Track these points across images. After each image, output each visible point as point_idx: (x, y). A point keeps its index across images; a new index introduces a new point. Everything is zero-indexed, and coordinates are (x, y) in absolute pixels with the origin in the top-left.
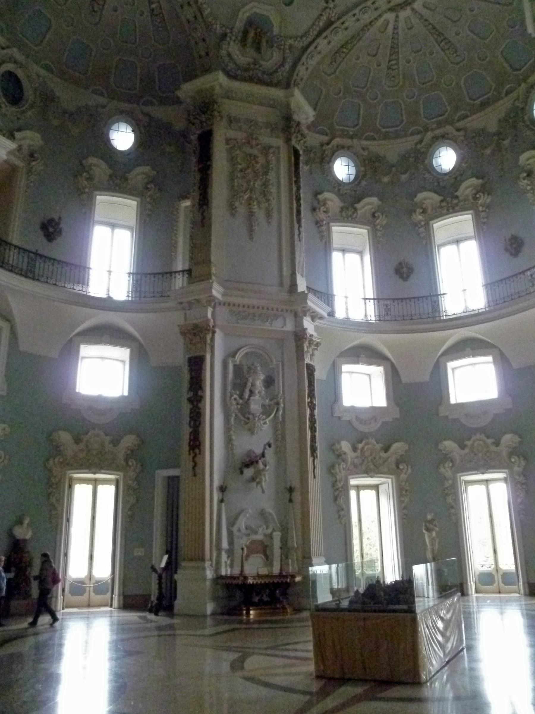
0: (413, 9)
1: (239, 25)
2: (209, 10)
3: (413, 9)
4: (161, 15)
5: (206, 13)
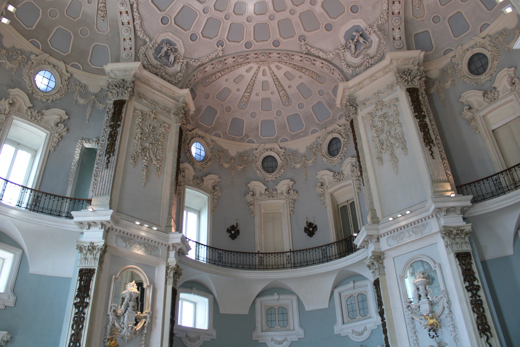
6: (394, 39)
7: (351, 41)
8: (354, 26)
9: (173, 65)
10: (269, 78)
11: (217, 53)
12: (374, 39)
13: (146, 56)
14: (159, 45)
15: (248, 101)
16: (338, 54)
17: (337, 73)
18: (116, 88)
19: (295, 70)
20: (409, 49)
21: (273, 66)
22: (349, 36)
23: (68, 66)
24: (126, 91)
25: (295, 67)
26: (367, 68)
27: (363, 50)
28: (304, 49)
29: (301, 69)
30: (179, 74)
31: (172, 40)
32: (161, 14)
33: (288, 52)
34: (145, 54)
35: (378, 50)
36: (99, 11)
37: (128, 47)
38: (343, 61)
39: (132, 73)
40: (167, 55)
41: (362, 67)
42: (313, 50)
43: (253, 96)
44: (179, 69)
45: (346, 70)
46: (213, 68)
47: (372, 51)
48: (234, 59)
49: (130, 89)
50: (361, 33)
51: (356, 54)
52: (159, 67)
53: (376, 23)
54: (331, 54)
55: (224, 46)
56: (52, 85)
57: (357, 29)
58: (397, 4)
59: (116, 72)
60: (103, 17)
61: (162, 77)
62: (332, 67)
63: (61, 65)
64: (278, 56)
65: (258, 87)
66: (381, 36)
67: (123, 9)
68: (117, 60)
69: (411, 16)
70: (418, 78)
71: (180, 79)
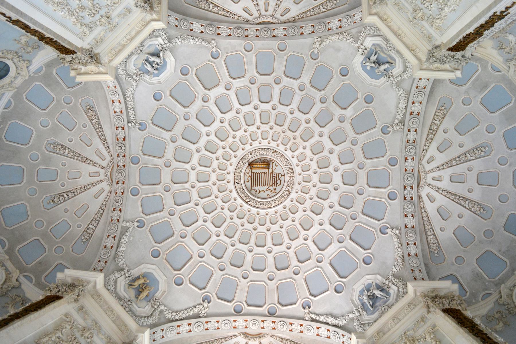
1: (136, 272)
4: (90, 235)
5: (121, 249)
9: (388, 293)
10: (446, 173)
11: (395, 236)
12: (369, 42)
15: (479, 204)
21: (428, 167)
22: (371, 74)
25: (430, 140)
27: (385, 54)
28: (398, 128)
29: (433, 131)
30: (400, 290)
33: (404, 148)
34: (362, 324)
40: (373, 298)
43: (475, 196)
44: (396, 288)
46: (415, 244)
51: (392, 62)
58: (330, 26)
64: (410, 160)
65: (459, 189)
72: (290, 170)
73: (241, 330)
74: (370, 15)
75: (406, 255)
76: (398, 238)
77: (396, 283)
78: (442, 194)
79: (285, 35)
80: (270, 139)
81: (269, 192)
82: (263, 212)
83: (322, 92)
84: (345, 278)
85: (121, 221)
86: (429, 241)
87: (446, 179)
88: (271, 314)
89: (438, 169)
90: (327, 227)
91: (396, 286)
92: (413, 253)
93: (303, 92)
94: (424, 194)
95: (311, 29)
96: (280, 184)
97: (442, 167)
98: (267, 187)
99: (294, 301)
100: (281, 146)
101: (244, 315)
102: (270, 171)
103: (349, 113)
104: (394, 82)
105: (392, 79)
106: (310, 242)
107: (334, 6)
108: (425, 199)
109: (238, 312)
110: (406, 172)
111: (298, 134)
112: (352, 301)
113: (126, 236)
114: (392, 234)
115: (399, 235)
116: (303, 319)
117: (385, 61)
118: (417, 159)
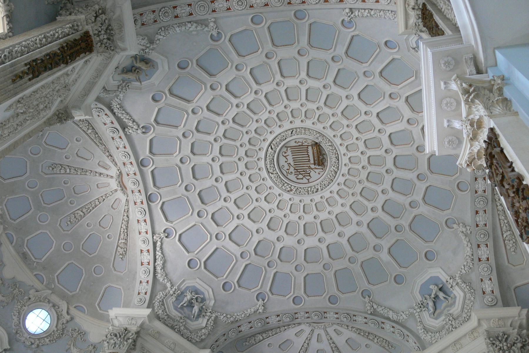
0: (116, 191)
1: (153, 56)
2: (179, 32)
3: (116, 191)
6: (484, 293)
7: (428, 297)
8: (431, 277)
12: (458, 293)
13: (163, 304)
14: (182, 293)
16: (412, 315)
17: (412, 339)
18: (115, 338)
19: (359, 336)
20: (506, 304)
21: (330, 330)
22: (424, 289)
23: (71, 308)
24: (125, 342)
25: (359, 331)
26: (449, 332)
27: (445, 309)
28: (368, 308)
29: (367, 335)
30: (203, 331)
31: (198, 286)
32: (188, 256)
33: (348, 312)
34: (163, 301)
35: (463, 308)
36: (119, 248)
37: (144, 291)
38: (419, 324)
39: (140, 322)
40: (190, 305)
41: (444, 332)
42: (381, 309)
44: (204, 325)
45: (423, 336)
47: (456, 310)
48: (278, 319)
49: (130, 341)
50: (440, 286)
51: (435, 315)
52: (178, 319)
53: (459, 272)
54: (404, 316)
55: (265, 301)
56: (45, 326)
57: (435, 280)
58: (483, 247)
59: (121, 319)
60: (122, 254)
61: (179, 332)
62: (406, 332)
63: (64, 306)
66: (466, 290)
67: (144, 247)
68: (127, 305)
69: (507, 263)
70: (519, 345)
71: (203, 337)
72: (315, 190)
73: (124, 170)
74: (479, 320)
75: (238, 324)
76: (254, 312)
77: (209, 323)
78: (305, 342)
79: (476, 192)
80: (350, 166)
81: (287, 167)
82: (262, 164)
83: (407, 228)
84: (205, 268)
85: (215, 15)
86: (257, 336)
87: (320, 346)
88: (149, 199)
89: (329, 339)
90: (256, 238)
91: (207, 324)
92: (242, 328)
93: (407, 206)
94: (302, 327)
95: (481, 224)
96: (298, 179)
97: (331, 343)
98: (292, 163)
99: (170, 218)
100: (347, 169)
101: (141, 171)
102: (313, 166)
103: (384, 256)
104: (415, 312)
105: (418, 310)
106: (236, 222)
107: (508, 247)
108: (298, 328)
109: (141, 164)
110: (323, 313)
111: (359, 198)
112: (184, 281)
113: (196, 27)
114: (258, 306)
115: (258, 312)
116: (153, 233)
117: (437, 305)
118: (338, 321)
